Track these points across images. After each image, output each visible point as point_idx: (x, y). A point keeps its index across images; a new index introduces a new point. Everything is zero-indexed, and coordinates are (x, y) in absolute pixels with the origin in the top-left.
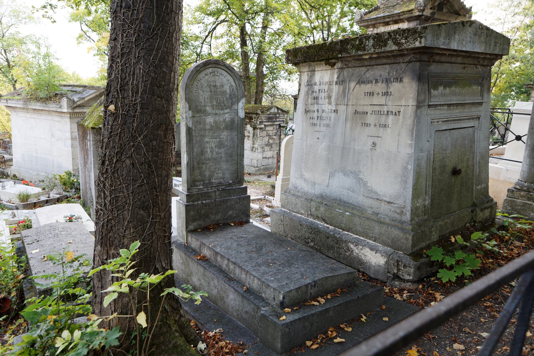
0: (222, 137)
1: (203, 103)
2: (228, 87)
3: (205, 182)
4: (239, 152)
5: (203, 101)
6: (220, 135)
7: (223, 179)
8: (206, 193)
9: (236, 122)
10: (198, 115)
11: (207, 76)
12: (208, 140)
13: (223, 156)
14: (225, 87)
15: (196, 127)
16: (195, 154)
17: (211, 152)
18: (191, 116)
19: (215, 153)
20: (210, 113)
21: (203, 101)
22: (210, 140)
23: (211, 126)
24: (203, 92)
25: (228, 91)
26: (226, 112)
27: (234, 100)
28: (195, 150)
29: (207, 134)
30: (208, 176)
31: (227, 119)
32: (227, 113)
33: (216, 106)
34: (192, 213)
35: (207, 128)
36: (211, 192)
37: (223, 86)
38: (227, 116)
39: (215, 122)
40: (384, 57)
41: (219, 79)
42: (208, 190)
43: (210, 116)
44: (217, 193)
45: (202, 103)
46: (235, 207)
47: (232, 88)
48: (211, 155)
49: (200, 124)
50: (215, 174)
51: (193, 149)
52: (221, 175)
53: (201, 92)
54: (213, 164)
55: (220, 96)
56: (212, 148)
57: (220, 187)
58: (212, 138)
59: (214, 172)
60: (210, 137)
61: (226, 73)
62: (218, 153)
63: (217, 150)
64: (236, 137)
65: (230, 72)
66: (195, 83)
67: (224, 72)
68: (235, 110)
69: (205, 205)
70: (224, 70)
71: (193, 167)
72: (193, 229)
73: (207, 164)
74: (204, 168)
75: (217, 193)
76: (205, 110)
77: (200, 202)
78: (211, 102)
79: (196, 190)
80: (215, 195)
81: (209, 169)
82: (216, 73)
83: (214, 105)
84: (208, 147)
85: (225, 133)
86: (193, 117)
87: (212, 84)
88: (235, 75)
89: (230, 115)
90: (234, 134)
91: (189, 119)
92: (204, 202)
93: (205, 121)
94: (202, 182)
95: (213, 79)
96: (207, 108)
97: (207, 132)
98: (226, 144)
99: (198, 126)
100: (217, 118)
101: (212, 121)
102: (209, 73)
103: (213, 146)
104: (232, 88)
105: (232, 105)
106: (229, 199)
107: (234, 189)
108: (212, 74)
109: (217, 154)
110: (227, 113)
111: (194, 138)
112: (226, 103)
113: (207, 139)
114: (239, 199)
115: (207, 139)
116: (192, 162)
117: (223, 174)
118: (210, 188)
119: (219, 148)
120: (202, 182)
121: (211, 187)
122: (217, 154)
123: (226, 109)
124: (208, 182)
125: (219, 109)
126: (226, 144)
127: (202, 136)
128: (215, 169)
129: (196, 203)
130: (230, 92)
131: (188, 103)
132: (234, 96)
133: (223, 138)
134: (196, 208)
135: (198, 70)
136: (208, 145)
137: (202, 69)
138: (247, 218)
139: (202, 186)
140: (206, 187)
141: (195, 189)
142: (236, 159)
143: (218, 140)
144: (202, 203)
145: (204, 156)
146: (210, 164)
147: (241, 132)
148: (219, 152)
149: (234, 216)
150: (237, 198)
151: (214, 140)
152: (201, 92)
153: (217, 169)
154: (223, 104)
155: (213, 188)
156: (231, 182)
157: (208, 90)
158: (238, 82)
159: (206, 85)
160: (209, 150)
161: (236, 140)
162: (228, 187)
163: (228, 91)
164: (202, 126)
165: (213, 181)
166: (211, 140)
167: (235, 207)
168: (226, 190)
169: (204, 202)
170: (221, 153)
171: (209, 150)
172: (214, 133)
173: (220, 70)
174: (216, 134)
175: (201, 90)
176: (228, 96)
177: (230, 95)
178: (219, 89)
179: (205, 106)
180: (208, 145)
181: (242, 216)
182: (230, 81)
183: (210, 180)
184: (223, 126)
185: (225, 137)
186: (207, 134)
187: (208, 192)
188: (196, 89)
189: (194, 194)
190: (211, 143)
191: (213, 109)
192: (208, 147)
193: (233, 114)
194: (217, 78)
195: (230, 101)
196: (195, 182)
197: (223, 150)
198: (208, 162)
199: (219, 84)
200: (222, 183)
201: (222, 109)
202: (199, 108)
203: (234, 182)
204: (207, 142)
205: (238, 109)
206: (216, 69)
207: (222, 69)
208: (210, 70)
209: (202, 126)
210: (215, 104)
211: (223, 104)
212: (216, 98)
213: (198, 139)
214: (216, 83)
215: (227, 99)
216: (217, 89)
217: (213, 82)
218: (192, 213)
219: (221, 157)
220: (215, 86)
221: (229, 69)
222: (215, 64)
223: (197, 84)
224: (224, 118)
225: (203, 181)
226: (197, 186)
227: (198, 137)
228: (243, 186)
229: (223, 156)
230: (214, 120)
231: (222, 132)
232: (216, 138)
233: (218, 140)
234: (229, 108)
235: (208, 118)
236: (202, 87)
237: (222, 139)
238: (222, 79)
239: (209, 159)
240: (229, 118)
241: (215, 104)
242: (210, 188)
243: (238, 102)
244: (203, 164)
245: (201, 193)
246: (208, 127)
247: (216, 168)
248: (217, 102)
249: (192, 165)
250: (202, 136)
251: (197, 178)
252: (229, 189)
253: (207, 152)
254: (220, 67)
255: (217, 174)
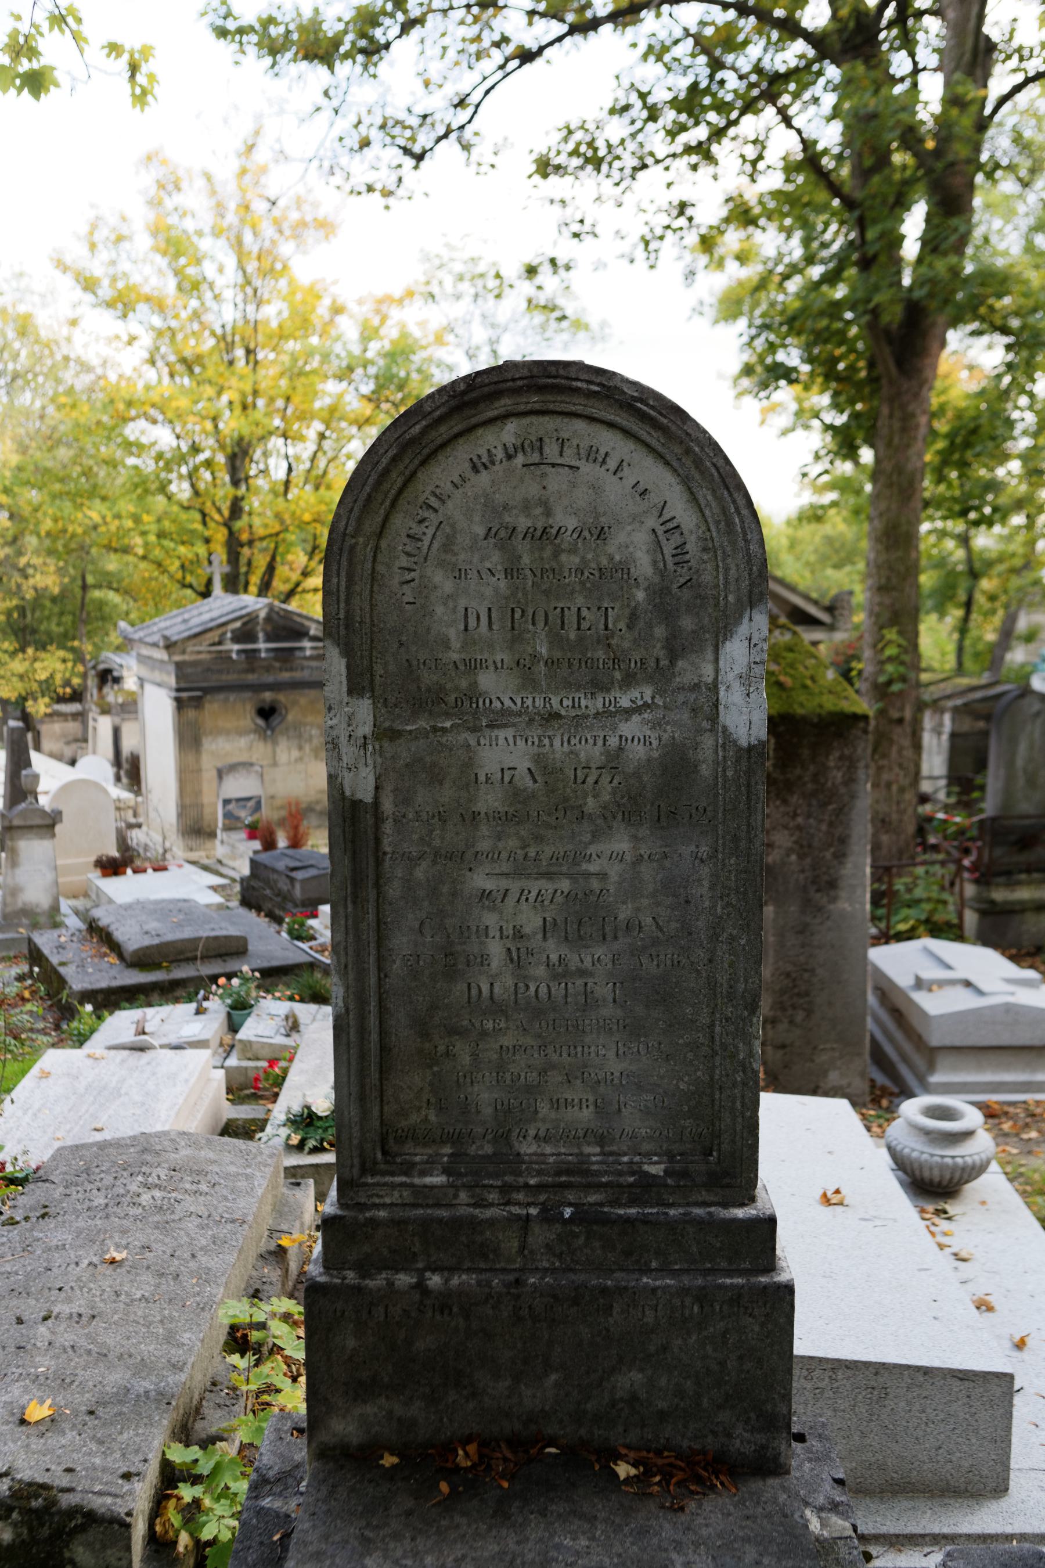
0: (593, 868)
1: (456, 644)
2: (641, 539)
3: (472, 1150)
4: (723, 978)
5: (453, 634)
6: (579, 857)
7: (601, 1140)
8: (456, 1224)
9: (705, 770)
10: (423, 723)
11: (484, 477)
12: (489, 885)
13: (603, 991)
14: (619, 538)
15: (404, 799)
16: (397, 967)
17: (517, 961)
18: (367, 729)
19: (541, 971)
20: (505, 712)
21: (453, 634)
22: (504, 884)
23: (516, 795)
24: (460, 574)
25: (643, 566)
26: (625, 702)
27: (687, 623)
28: (401, 943)
29: (484, 845)
30: (488, 1111)
31: (638, 752)
32: (638, 710)
33: (550, 663)
34: (351, 1343)
35: (481, 807)
36: (492, 1222)
37: (602, 534)
38: (630, 728)
39: (543, 767)
40: (724, 510)
41: (573, 485)
42: (481, 1203)
43: (509, 733)
44: (540, 1236)
45: (446, 645)
46: (665, 1348)
47: (676, 539)
48: (510, 982)
49: (436, 778)
50: (544, 1109)
51: (380, 941)
52: (586, 1115)
53: (442, 581)
54: (529, 1041)
55: (580, 601)
56: (519, 935)
57: (571, 1197)
58: (517, 873)
59: (530, 1089)
60: (506, 867)
61: (631, 445)
62: (560, 973)
63: (553, 950)
64: (705, 871)
65: (654, 438)
66: (400, 523)
67: (608, 441)
68: (696, 687)
69: (444, 1302)
70: (611, 425)
71: (384, 1049)
72: (355, 1441)
73: (484, 1034)
74: (467, 1060)
75: (540, 1236)
76: (473, 694)
77: (404, 1280)
78: (516, 637)
79: (395, 1197)
80: (522, 1248)
81: (500, 1067)
82: (551, 451)
83: (535, 657)
84: (494, 932)
85: (621, 843)
86: (385, 734)
87: (523, 523)
88: (688, 451)
89: (656, 725)
90: (687, 850)
91: (349, 752)
92: (435, 1280)
93: (469, 764)
94: (447, 1150)
95: (532, 490)
96: (486, 680)
97: (484, 830)
98: (625, 913)
99: (422, 797)
100: (560, 747)
101: (523, 765)
102: (500, 454)
103: (531, 921)
104: (676, 539)
105: (673, 656)
106: (622, 1290)
107: (672, 1226)
108: (520, 459)
109: (555, 977)
110: (638, 710)
111: (395, 872)
112: (624, 641)
113: (480, 880)
114: (702, 1297)
115: (480, 880)
116: (373, 1021)
117: (600, 1109)
118: (493, 1196)
119: (576, 939)
120: (447, 1150)
121: (506, 1189)
122: (555, 977)
123: (629, 681)
124: (489, 1149)
125: (568, 685)
126: (625, 913)
127: (450, 857)
128: (543, 1072)
129: (377, 1282)
130: (662, 573)
131: (347, 652)
132: (686, 594)
133: (603, 876)
134: (379, 1312)
135: (413, 441)
136: (490, 919)
137: (444, 431)
138: (761, 1438)
139: (447, 1171)
140: (469, 1187)
141: (393, 1186)
142: (704, 1019)
143: (565, 885)
144: (420, 1286)
145: (461, 987)
146: (507, 1041)
147: (736, 839)
148: (574, 961)
149: (662, 1405)
150: (684, 1291)
151: (535, 886)
152: (442, 581)
153: (555, 1077)
154: (600, 654)
155: (520, 1196)
156: (656, 1169)
157: (495, 559)
158: (719, 499)
159: (481, 531)
160: (496, 949)
161: (702, 891)
162: (632, 1202)
163: (643, 566)
164: (447, 794)
165: (528, 1148)
166: (515, 886)
167: (665, 1348)
168: (607, 1221)
169: (435, 1280)
170: (582, 973)
171: (496, 949)
172: (539, 839)
173: (580, 425)
174: (548, 851)
175: (441, 564)
176: (640, 595)
177: (660, 593)
178: (573, 551)
179: (473, 666)
180: (490, 919)
181: (724, 1416)
182: (654, 498)
183: (503, 1138)
184: (606, 797)
185: (614, 871)
186: (484, 845)
187: (474, 1224)
188: (404, 561)
189: (373, 1222)
190: (511, 901)
191: (529, 682)
192: (494, 932)
193: (685, 716)
194: (557, 481)
195: (660, 631)
196: (401, 1140)
197: (600, 951)
198: (489, 1025)
199: (571, 523)
200: (587, 1173)
201: (598, 686)
202: (428, 678)
203: (685, 1174)
204: (485, 895)
205: (714, 687)
206: (548, 424)
207: (592, 419)
208: (510, 432)
209: (447, 794)
210: (544, 651)
211: (600, 654)
212: (554, 616)
213: (419, 873)
214: (548, 513)
215: (633, 618)
216: (556, 554)
217: (526, 507)
218: (351, 1343)
219: (589, 1001)
220: (543, 536)
221: (643, 417)
222: (541, 389)
223: (417, 529)
224: (613, 741)
225: (456, 1139)
226: (408, 1169)
227: (424, 864)
228: (740, 1213)
229: (603, 991)
230: (538, 759)
231: (595, 836)
232: (549, 875)
233: (565, 885)
234: (650, 679)
235: (493, 743)
236: (448, 546)
237: (595, 884)
238: (595, 488)
239: (497, 1008)
240: (646, 741)
241: (544, 651)
242: (493, 1196)
243: (723, 631)
244: (454, 1031)
245: (426, 1223)
246: (489, 800)
247: (553, 1066)
248: (556, 640)
249: (374, 1037)
250: (450, 857)
251: (414, 1118)
252: (628, 1220)
253: (484, 959)
254: (578, 405)
255: (556, 1104)
